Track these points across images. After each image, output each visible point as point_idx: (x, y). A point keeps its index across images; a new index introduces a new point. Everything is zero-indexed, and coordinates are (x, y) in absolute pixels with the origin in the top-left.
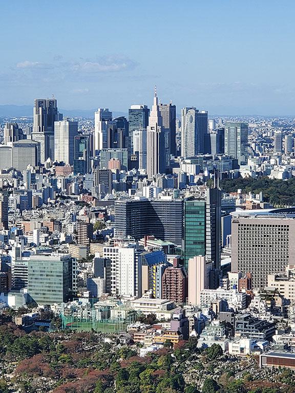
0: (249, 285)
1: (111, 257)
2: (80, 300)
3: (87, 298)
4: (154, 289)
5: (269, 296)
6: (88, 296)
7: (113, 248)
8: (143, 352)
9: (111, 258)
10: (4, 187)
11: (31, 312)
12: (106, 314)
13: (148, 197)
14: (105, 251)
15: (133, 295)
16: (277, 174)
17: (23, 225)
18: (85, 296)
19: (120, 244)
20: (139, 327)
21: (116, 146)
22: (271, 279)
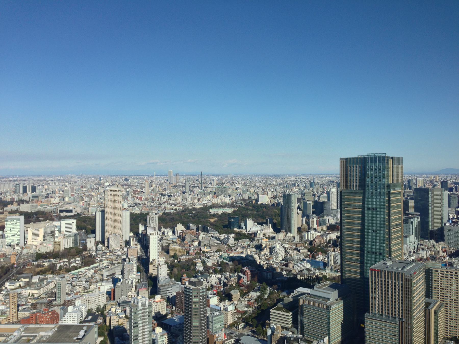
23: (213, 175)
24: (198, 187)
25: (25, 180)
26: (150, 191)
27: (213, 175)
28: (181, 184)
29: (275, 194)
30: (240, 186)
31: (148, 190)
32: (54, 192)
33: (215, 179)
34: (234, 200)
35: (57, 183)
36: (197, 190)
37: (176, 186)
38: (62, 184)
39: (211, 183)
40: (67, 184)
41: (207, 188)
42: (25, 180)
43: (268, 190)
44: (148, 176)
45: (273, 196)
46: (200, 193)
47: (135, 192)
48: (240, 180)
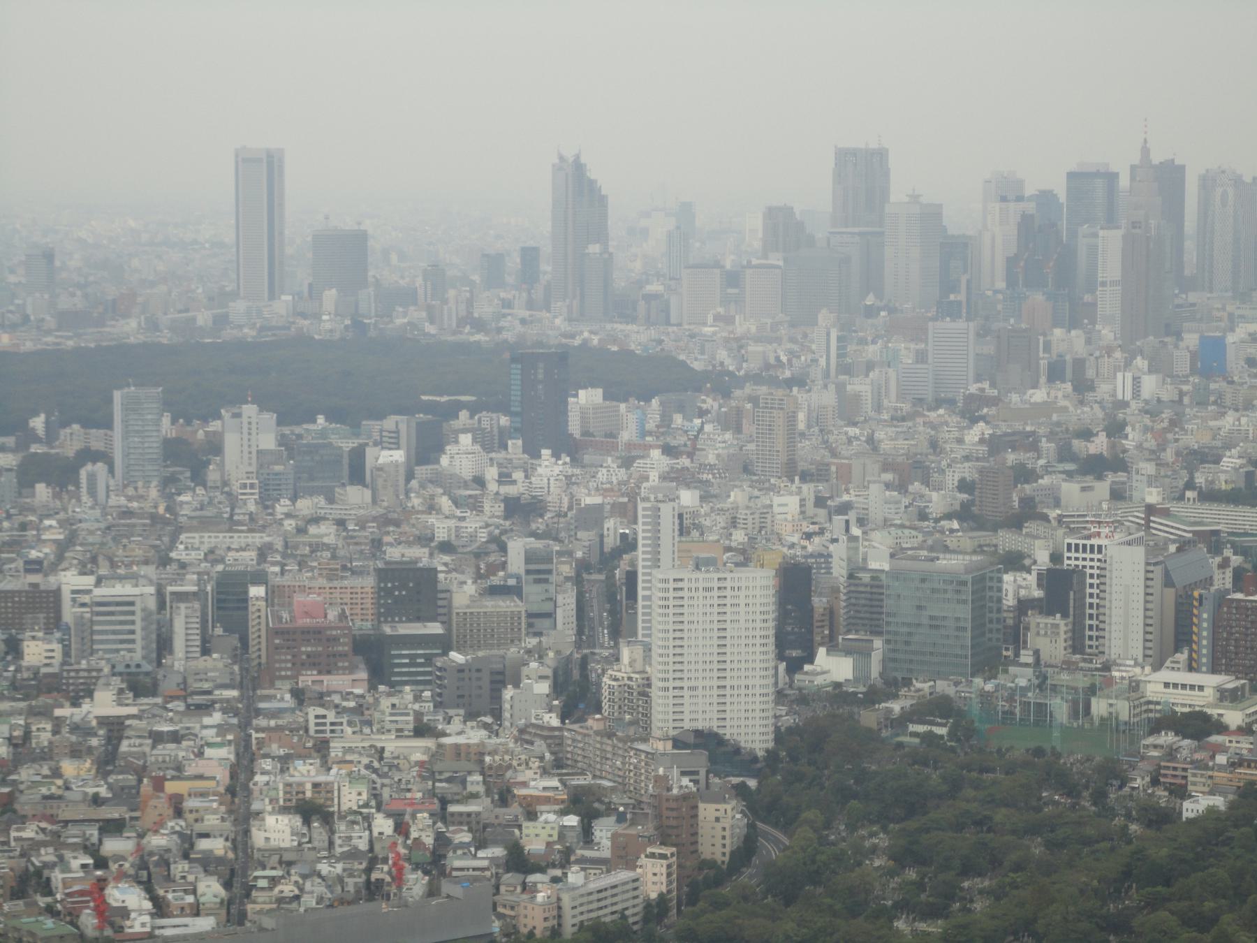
1: (1084, 563)
2: (1012, 669)
3: (1027, 665)
4: (1195, 647)
6: (1030, 660)
7: (1088, 542)
8: (1191, 809)
9: (1084, 567)
10: (768, 366)
11: (895, 697)
13: (1128, 396)
14: (1069, 550)
15: (1140, 659)
17: (833, 468)
18: (1023, 659)
19: (1105, 531)
20: (1170, 747)
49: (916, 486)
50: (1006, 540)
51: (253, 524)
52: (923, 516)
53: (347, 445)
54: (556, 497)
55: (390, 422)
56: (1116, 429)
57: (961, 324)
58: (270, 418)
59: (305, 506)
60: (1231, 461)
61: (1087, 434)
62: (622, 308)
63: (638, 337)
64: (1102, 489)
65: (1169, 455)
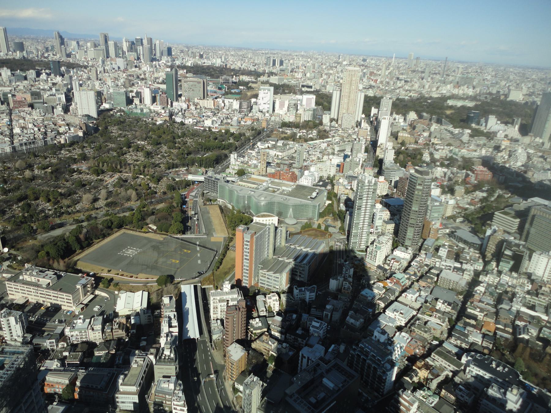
0: (189, 101)
5: (196, 105)
8: (158, 123)
12: (142, 110)
16: (189, 64)
21: (132, 52)
22: (196, 99)
23: (459, 62)
24: (439, 74)
25: (275, 54)
26: (387, 74)
27: (459, 62)
28: (420, 70)
29: (531, 91)
30: (489, 77)
31: (385, 73)
32: (298, 67)
33: (461, 66)
34: (478, 92)
35: (300, 59)
36: (438, 77)
37: (414, 71)
38: (304, 59)
39: (454, 71)
40: (309, 60)
41: (449, 76)
42: (275, 54)
43: (523, 85)
44: (386, 57)
45: (528, 93)
46: (440, 81)
47: (372, 73)
48: (491, 69)
49: (116, 82)
50: (130, 89)
51: (8, 86)
52: (118, 85)
53: (24, 75)
54: (60, 82)
55: (31, 71)
56: (145, 74)
57: (121, 59)
58: (9, 71)
59: (17, 83)
60: (161, 79)
61: (141, 75)
62: (69, 55)
63: (71, 60)
64: (144, 82)
65: (152, 78)
